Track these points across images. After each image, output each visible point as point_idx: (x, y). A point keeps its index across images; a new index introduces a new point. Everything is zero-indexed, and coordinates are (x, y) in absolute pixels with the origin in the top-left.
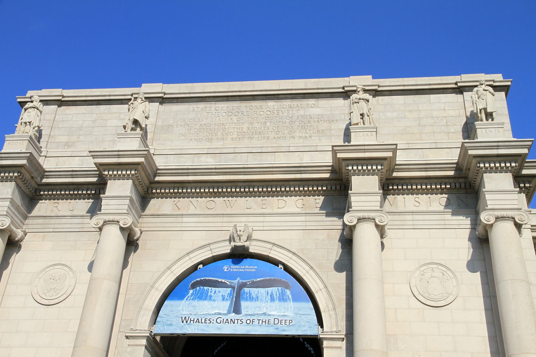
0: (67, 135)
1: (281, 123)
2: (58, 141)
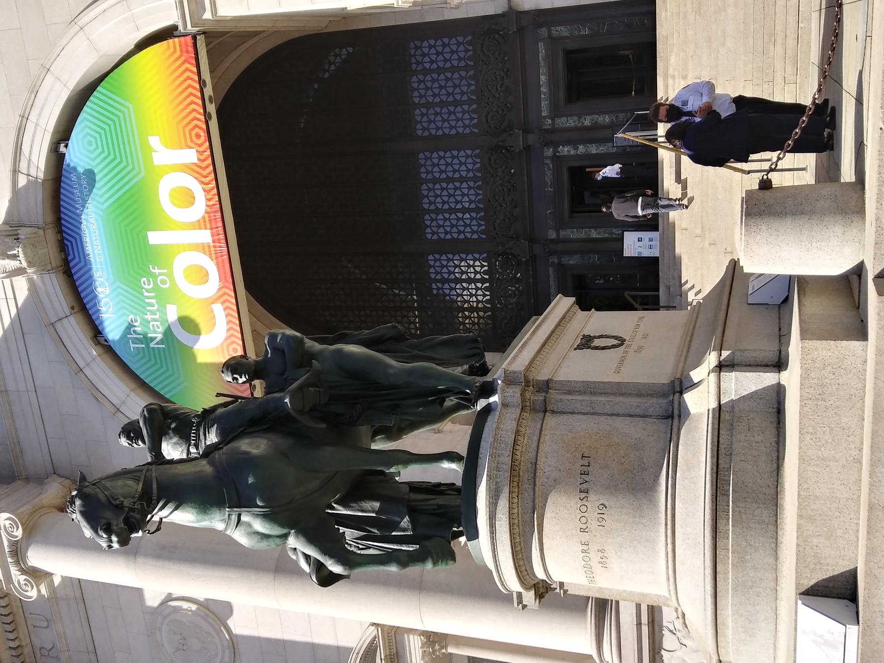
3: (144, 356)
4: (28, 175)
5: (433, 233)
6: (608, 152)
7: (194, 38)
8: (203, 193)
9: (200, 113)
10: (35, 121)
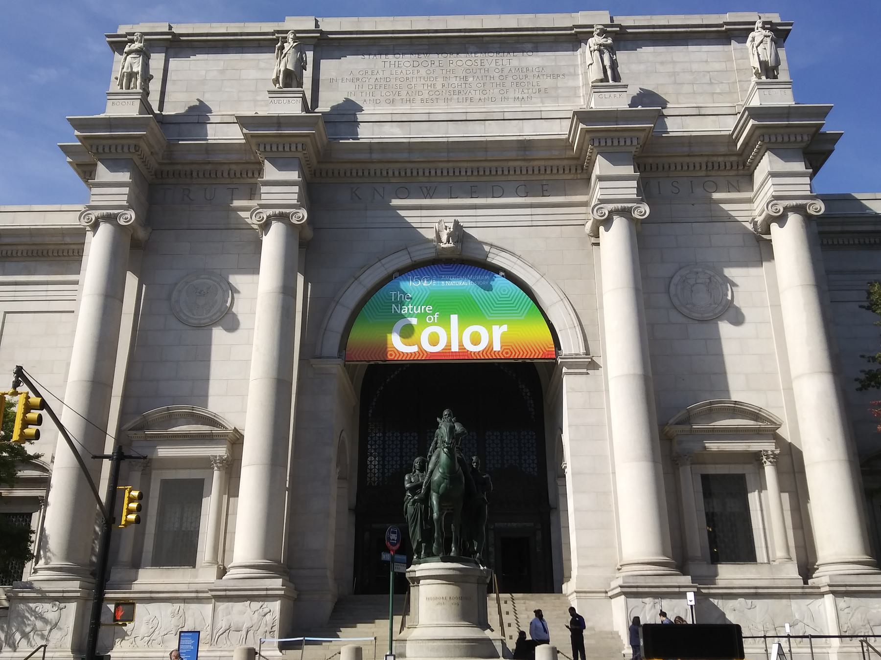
0: (186, 92)
1: (488, 78)
2: (174, 100)
3: (387, 299)
7: (554, 359)
8: (478, 350)
9: (518, 356)
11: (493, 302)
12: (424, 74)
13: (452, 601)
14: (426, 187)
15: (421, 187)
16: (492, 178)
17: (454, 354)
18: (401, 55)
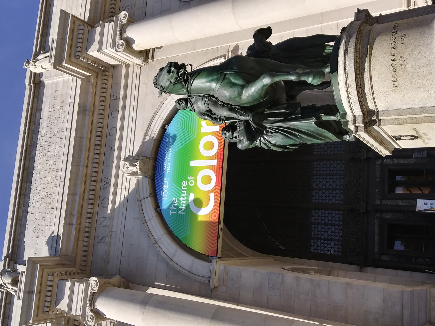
4: (150, 136)
5: (316, 199)
6: (409, 163)
10: (160, 117)
11: (185, 132)
12: (42, 186)
13: (398, 44)
14: (104, 184)
15: (104, 189)
16: (104, 136)
17: (219, 163)
18: (30, 202)
